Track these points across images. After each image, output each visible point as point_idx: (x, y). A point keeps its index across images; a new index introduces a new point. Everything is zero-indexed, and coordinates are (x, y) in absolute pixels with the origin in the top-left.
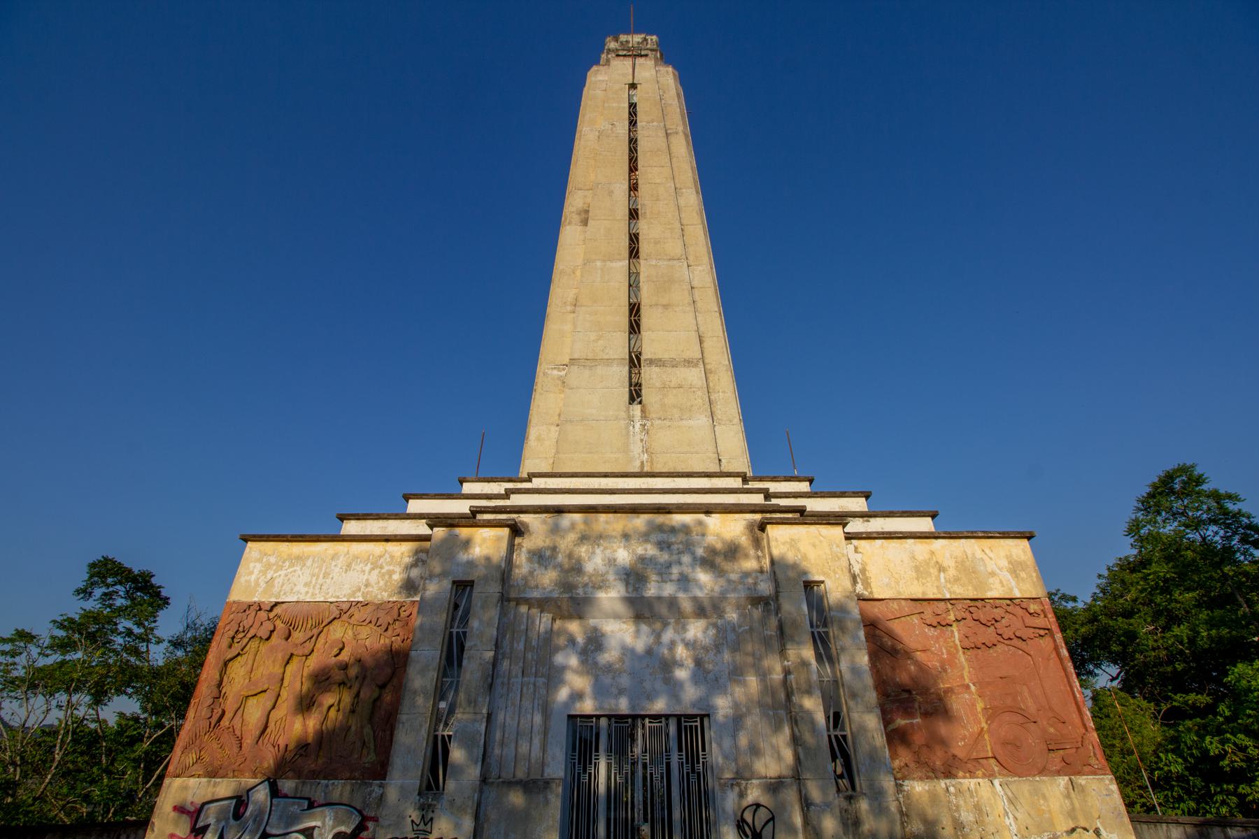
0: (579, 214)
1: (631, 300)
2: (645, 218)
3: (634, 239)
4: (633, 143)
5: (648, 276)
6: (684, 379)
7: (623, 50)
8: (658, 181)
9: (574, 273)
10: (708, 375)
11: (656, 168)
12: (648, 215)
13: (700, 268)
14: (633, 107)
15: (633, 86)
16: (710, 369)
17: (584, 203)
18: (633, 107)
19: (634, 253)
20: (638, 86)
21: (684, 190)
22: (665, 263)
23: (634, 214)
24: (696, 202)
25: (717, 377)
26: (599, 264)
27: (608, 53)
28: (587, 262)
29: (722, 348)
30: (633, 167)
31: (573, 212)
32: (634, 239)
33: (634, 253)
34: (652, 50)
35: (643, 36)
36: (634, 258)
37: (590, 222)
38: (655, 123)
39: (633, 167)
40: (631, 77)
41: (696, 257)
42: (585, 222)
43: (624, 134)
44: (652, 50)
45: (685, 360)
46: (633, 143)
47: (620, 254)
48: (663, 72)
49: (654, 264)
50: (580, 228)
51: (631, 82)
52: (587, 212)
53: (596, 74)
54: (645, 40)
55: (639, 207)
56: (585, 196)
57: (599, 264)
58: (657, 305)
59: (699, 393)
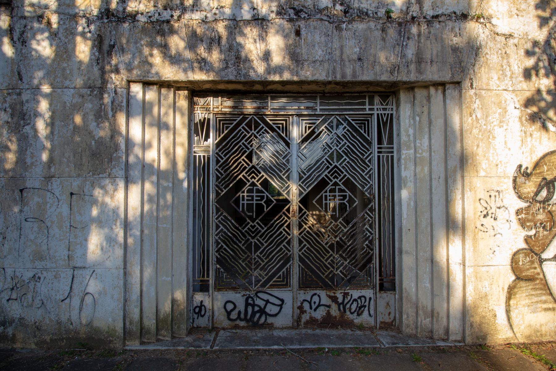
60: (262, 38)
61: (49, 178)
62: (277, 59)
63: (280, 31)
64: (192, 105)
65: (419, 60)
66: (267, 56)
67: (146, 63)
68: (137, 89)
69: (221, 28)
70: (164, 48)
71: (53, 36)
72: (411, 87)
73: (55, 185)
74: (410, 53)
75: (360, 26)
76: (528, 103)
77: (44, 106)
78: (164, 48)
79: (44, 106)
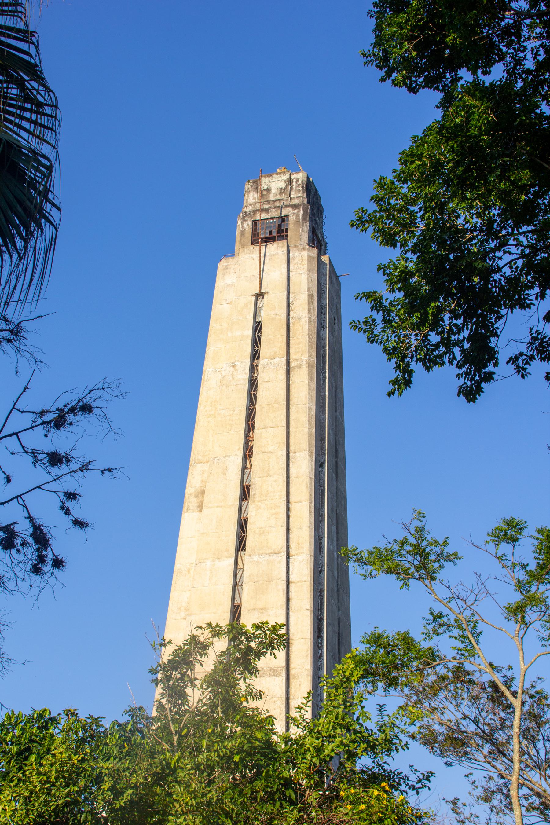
0: (197, 497)
1: (236, 602)
2: (254, 502)
5: (249, 576)
6: (268, 688)
7: (262, 210)
8: (271, 448)
9: (189, 572)
10: (292, 681)
11: (270, 430)
12: (257, 496)
13: (300, 558)
14: (258, 326)
15: (260, 295)
16: (294, 675)
17: (202, 482)
18: (258, 326)
19: (241, 545)
20: (265, 296)
21: (297, 454)
22: (266, 558)
24: (307, 471)
25: (298, 683)
26: (209, 563)
27: (244, 220)
29: (307, 651)
30: (250, 427)
31: (191, 494)
33: (241, 545)
34: (295, 206)
35: (287, 176)
36: (242, 550)
37: (204, 510)
38: (277, 360)
39: (250, 427)
40: (258, 289)
41: (298, 544)
42: (200, 507)
43: (243, 379)
44: (295, 206)
45: (271, 669)
47: (227, 551)
48: (297, 260)
49: (256, 560)
50: (196, 515)
51: (258, 292)
52: (203, 492)
53: (224, 274)
54: (290, 182)
55: (251, 483)
56: (203, 472)
57: (209, 563)
58: (255, 609)
59: (278, 703)
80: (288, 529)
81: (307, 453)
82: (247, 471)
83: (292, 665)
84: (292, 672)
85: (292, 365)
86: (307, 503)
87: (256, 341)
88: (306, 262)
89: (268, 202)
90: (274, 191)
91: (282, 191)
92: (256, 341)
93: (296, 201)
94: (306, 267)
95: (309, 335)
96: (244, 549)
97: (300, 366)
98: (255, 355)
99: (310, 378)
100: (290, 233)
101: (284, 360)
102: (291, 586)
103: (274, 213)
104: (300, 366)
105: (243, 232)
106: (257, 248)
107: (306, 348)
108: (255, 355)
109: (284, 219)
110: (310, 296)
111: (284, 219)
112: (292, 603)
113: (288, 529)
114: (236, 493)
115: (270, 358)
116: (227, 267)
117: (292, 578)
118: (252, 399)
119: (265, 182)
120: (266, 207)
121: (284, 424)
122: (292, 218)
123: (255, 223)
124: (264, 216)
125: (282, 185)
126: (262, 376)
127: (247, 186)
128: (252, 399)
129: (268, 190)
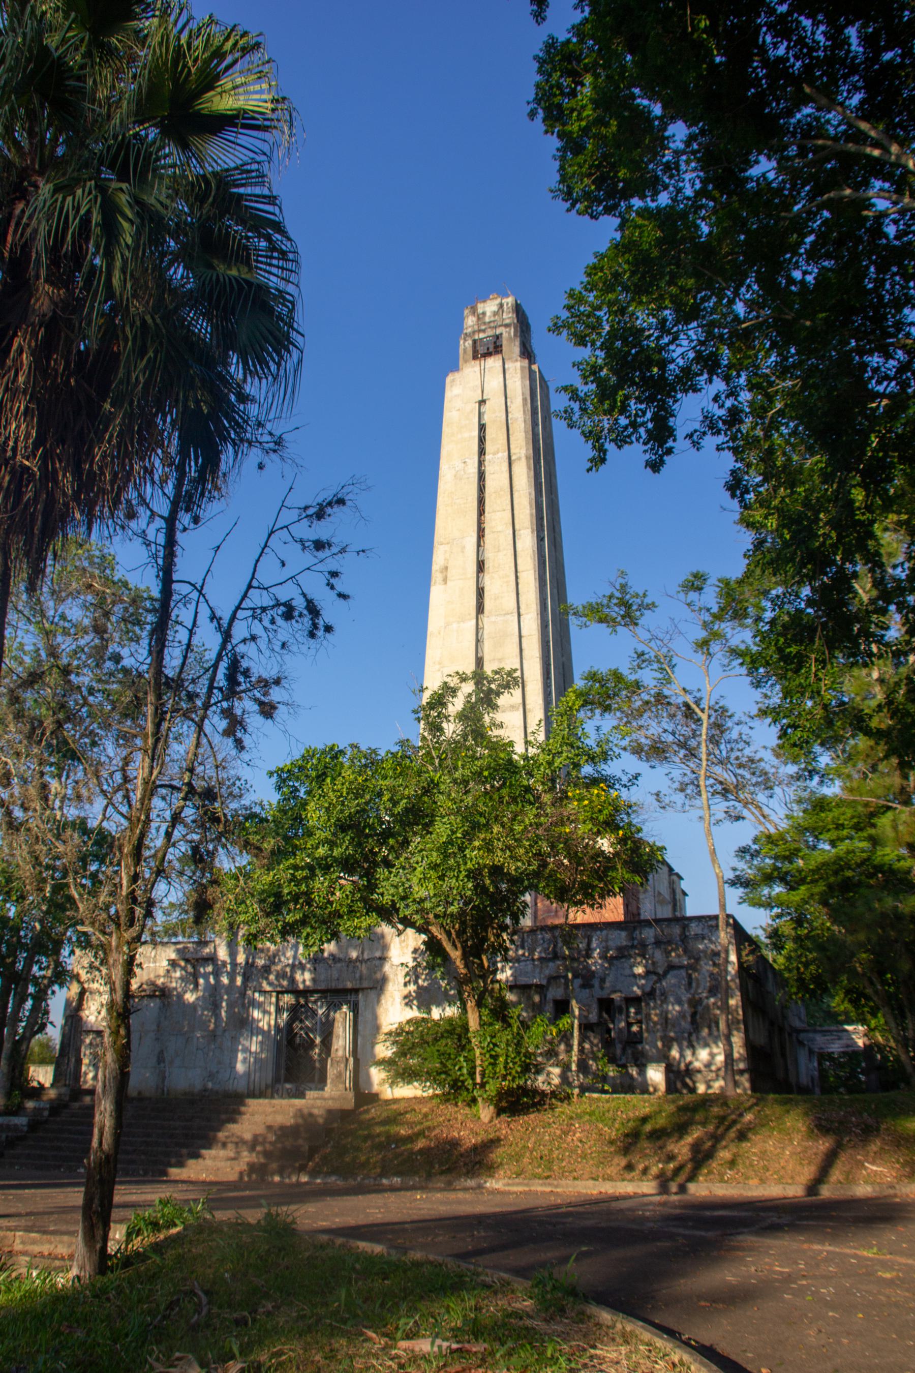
3: (480, 593)
4: (481, 476)
7: (480, 331)
8: (499, 528)
14: (482, 428)
15: (482, 402)
18: (482, 428)
19: (480, 608)
23: (481, 567)
26: (455, 625)
27: (465, 340)
28: (447, 625)
30: (481, 512)
32: (480, 593)
33: (480, 608)
34: (507, 326)
35: (498, 301)
38: (500, 455)
39: (481, 512)
42: (445, 580)
44: (507, 326)
46: (481, 476)
50: (442, 587)
52: (446, 568)
57: (455, 625)
60: (303, 974)
61: (225, 1031)
62: (308, 983)
63: (310, 970)
64: (278, 999)
65: (361, 978)
66: (304, 981)
67: (260, 984)
68: (257, 995)
69: (288, 970)
70: (267, 979)
71: (228, 973)
72: (363, 989)
73: (227, 1034)
74: (357, 975)
75: (339, 965)
76: (405, 997)
77: (224, 1004)
78: (267, 979)
79: (224, 1004)
80: (518, 594)
81: (529, 530)
82: (481, 549)
83: (527, 702)
84: (528, 707)
85: (513, 458)
86: (532, 572)
87: (482, 440)
88: (519, 371)
89: (485, 323)
90: (488, 314)
91: (495, 314)
92: (482, 440)
93: (507, 321)
94: (519, 375)
95: (526, 432)
96: (483, 612)
97: (519, 459)
98: (482, 452)
99: (529, 468)
100: (504, 348)
101: (506, 454)
102: (523, 640)
103: (490, 332)
104: (519, 459)
105: (465, 351)
106: (477, 362)
107: (524, 443)
108: (482, 452)
109: (498, 337)
110: (524, 400)
111: (498, 337)
112: (525, 653)
113: (518, 594)
114: (473, 567)
115: (494, 454)
116: (453, 381)
117: (523, 633)
118: (481, 489)
119: (481, 308)
120: (483, 327)
121: (509, 507)
122: (505, 335)
123: (475, 342)
124: (482, 335)
125: (495, 308)
126: (489, 469)
127: (466, 312)
128: (481, 489)
129: (484, 314)
